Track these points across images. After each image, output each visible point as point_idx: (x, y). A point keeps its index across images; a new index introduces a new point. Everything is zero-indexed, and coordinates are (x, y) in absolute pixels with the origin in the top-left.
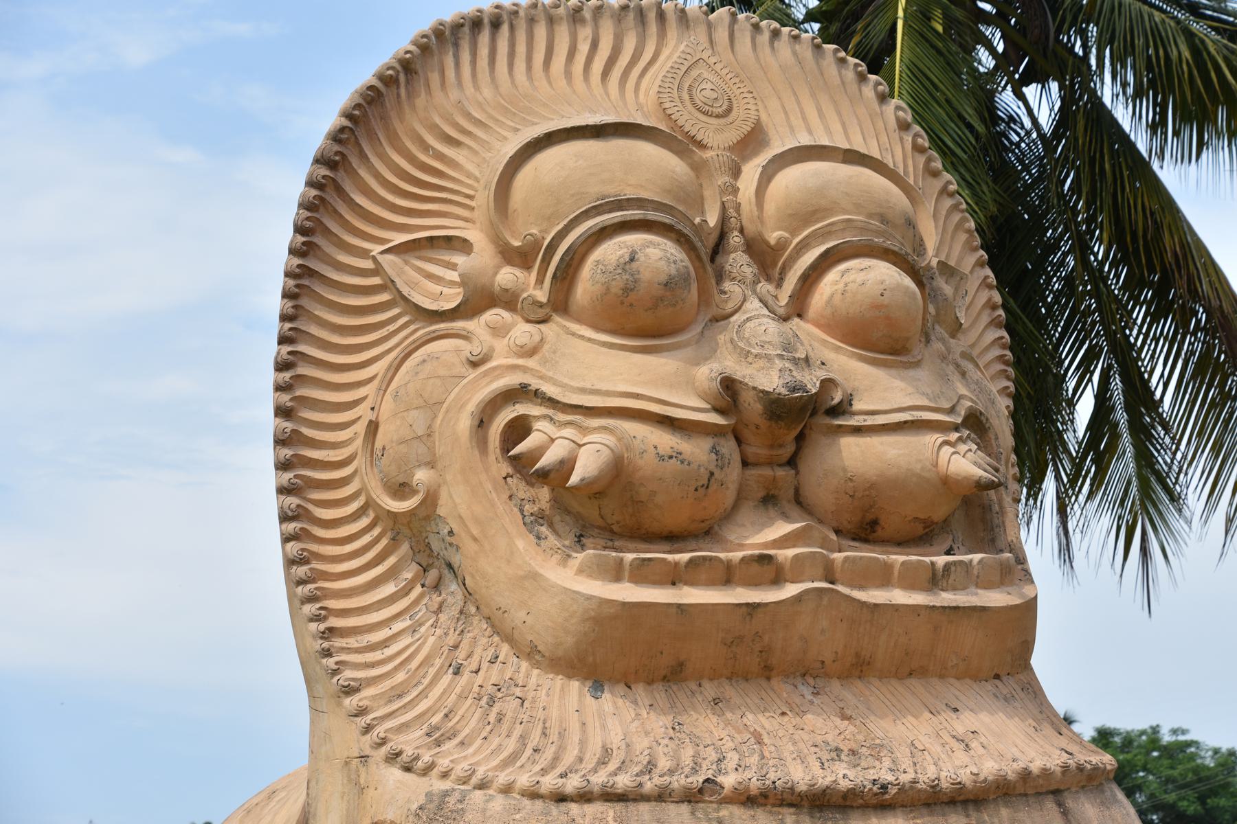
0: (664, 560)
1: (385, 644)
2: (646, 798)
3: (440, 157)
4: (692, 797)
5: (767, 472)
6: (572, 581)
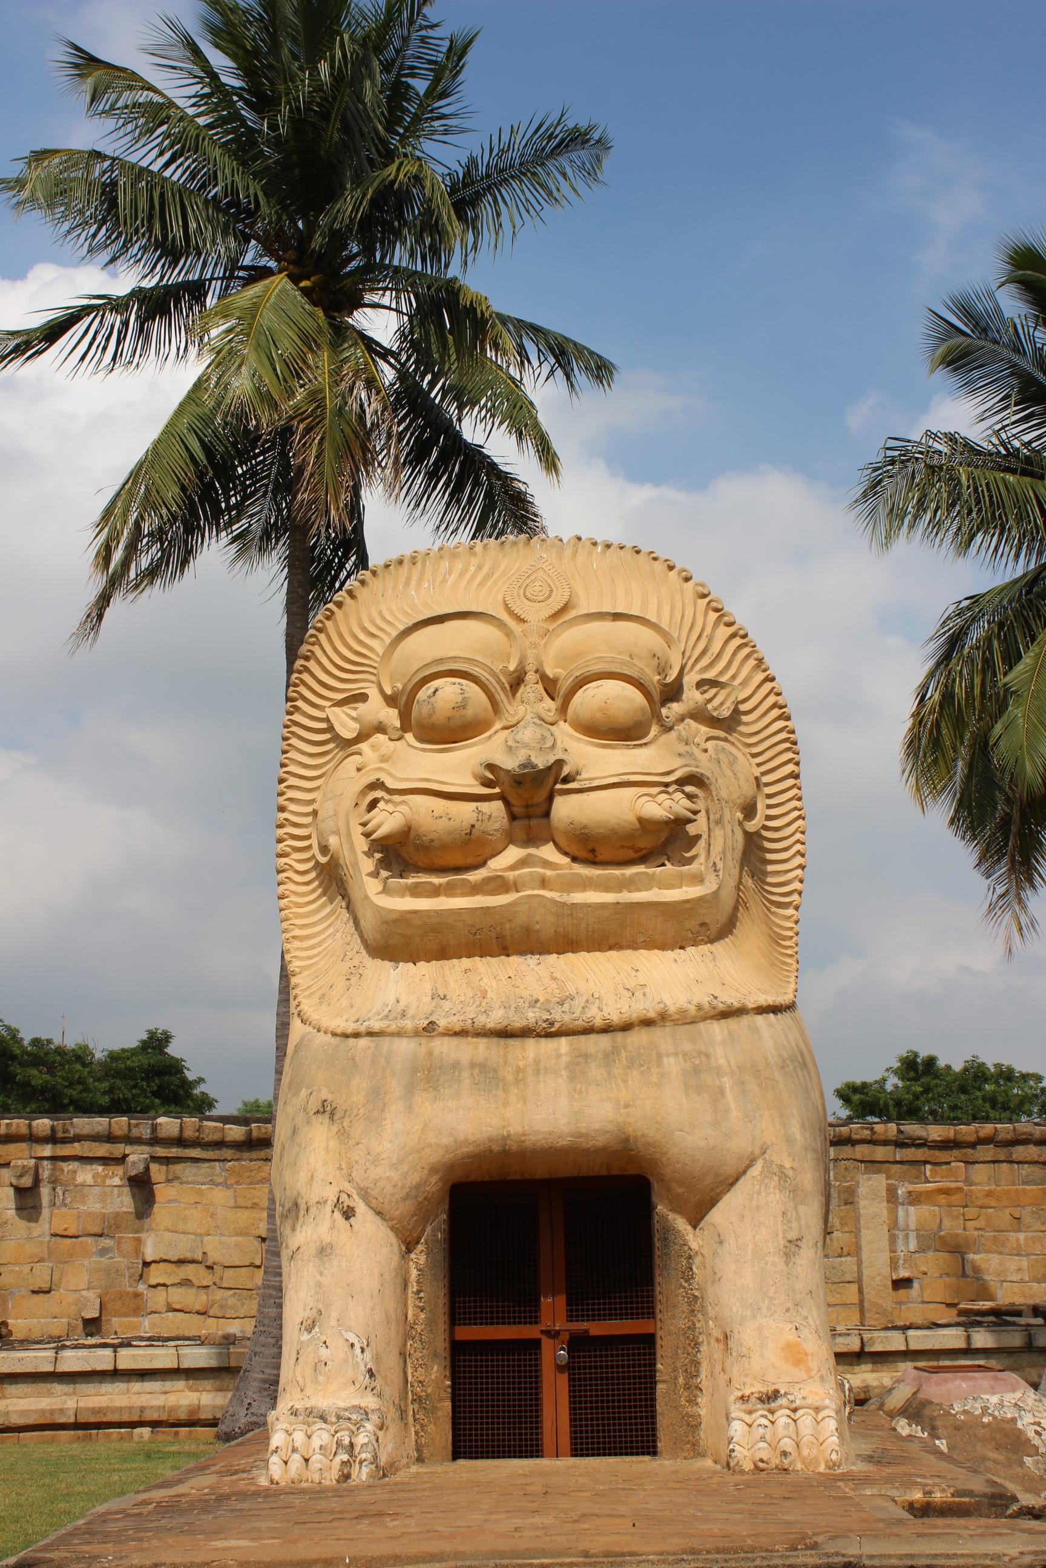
0: (430, 883)
1: (319, 944)
2: (392, 1035)
3: (366, 646)
6: (385, 897)
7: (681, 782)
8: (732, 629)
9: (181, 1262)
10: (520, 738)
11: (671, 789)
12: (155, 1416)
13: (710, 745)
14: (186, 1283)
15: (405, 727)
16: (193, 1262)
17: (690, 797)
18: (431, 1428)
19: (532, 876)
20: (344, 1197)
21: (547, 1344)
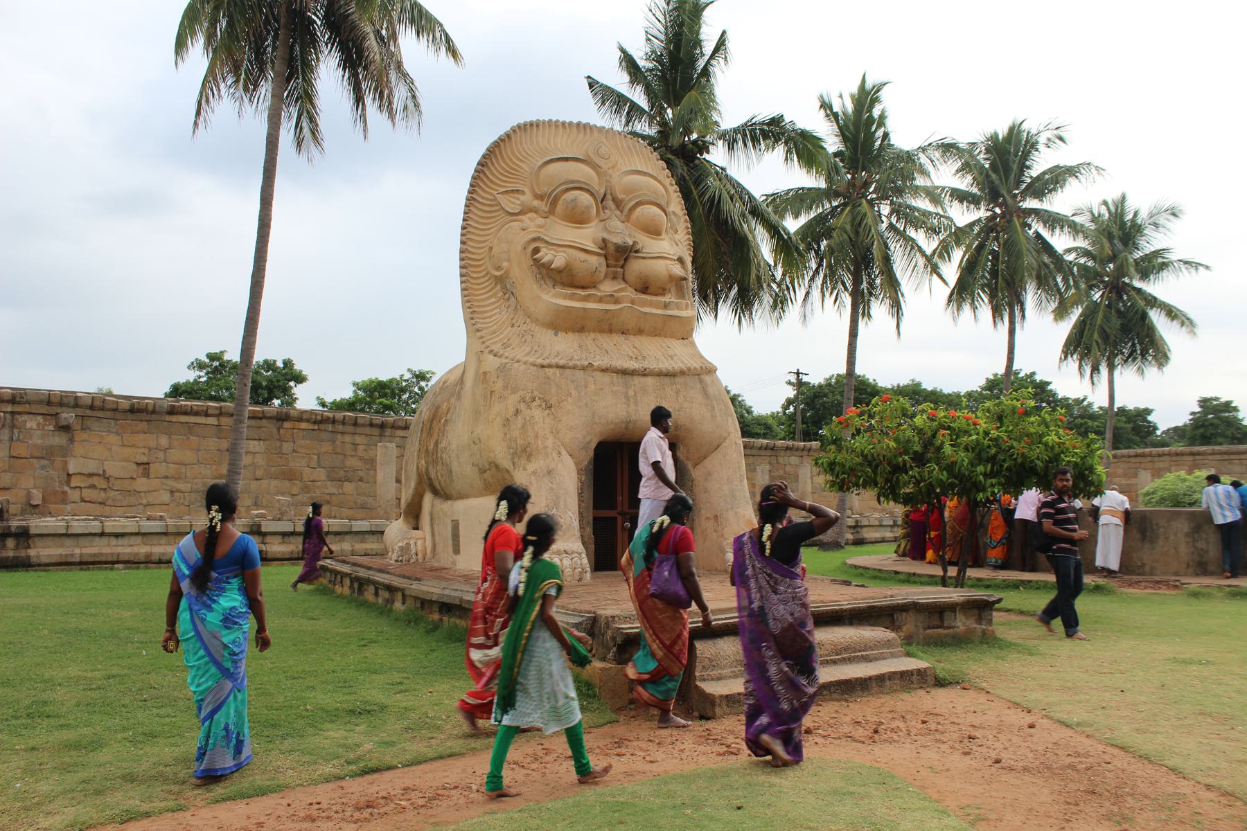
4: (584, 368)
9: (91, 475)
12: (126, 558)
14: (93, 487)
16: (98, 475)
21: (619, 519)
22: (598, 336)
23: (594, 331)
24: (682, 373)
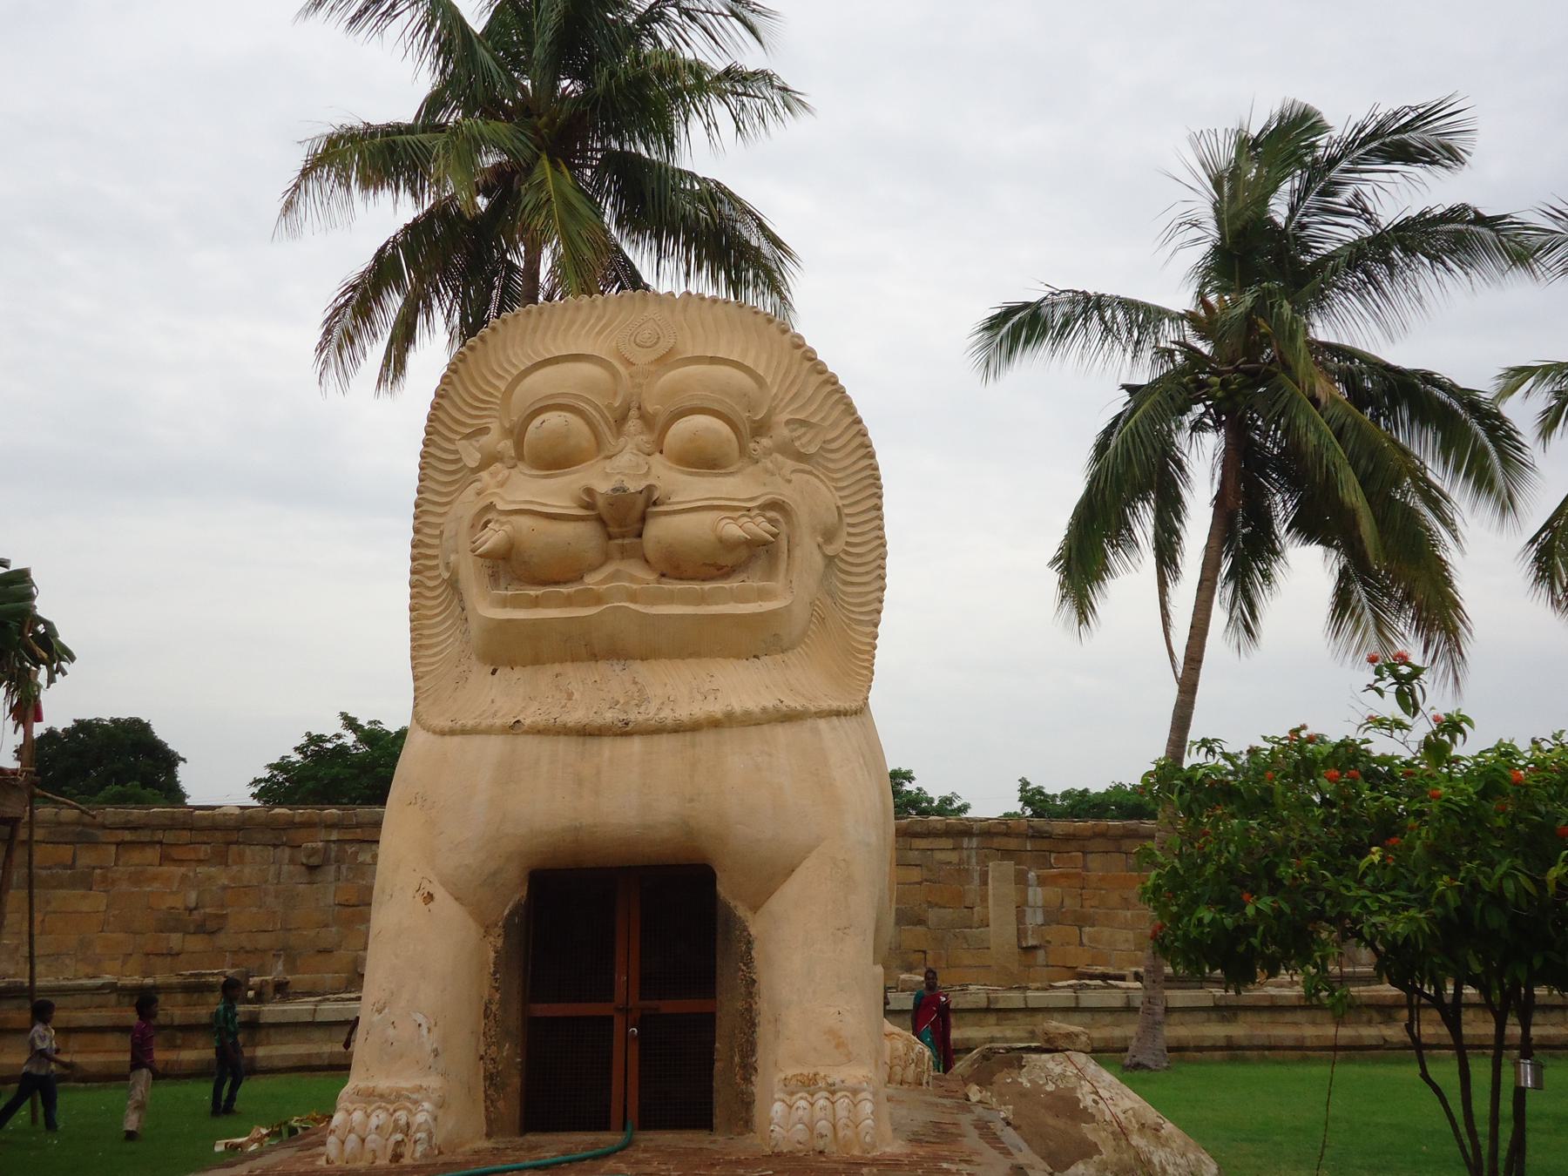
1: (441, 652)
5: (620, 541)
7: (764, 507)
8: (824, 377)
10: (621, 469)
11: (753, 513)
13: (794, 477)
15: (520, 457)
17: (771, 521)
18: (501, 1104)
19: (624, 592)
20: (425, 883)
21: (619, 1023)
22: (569, 668)
23: (562, 661)
24: (715, 724)
